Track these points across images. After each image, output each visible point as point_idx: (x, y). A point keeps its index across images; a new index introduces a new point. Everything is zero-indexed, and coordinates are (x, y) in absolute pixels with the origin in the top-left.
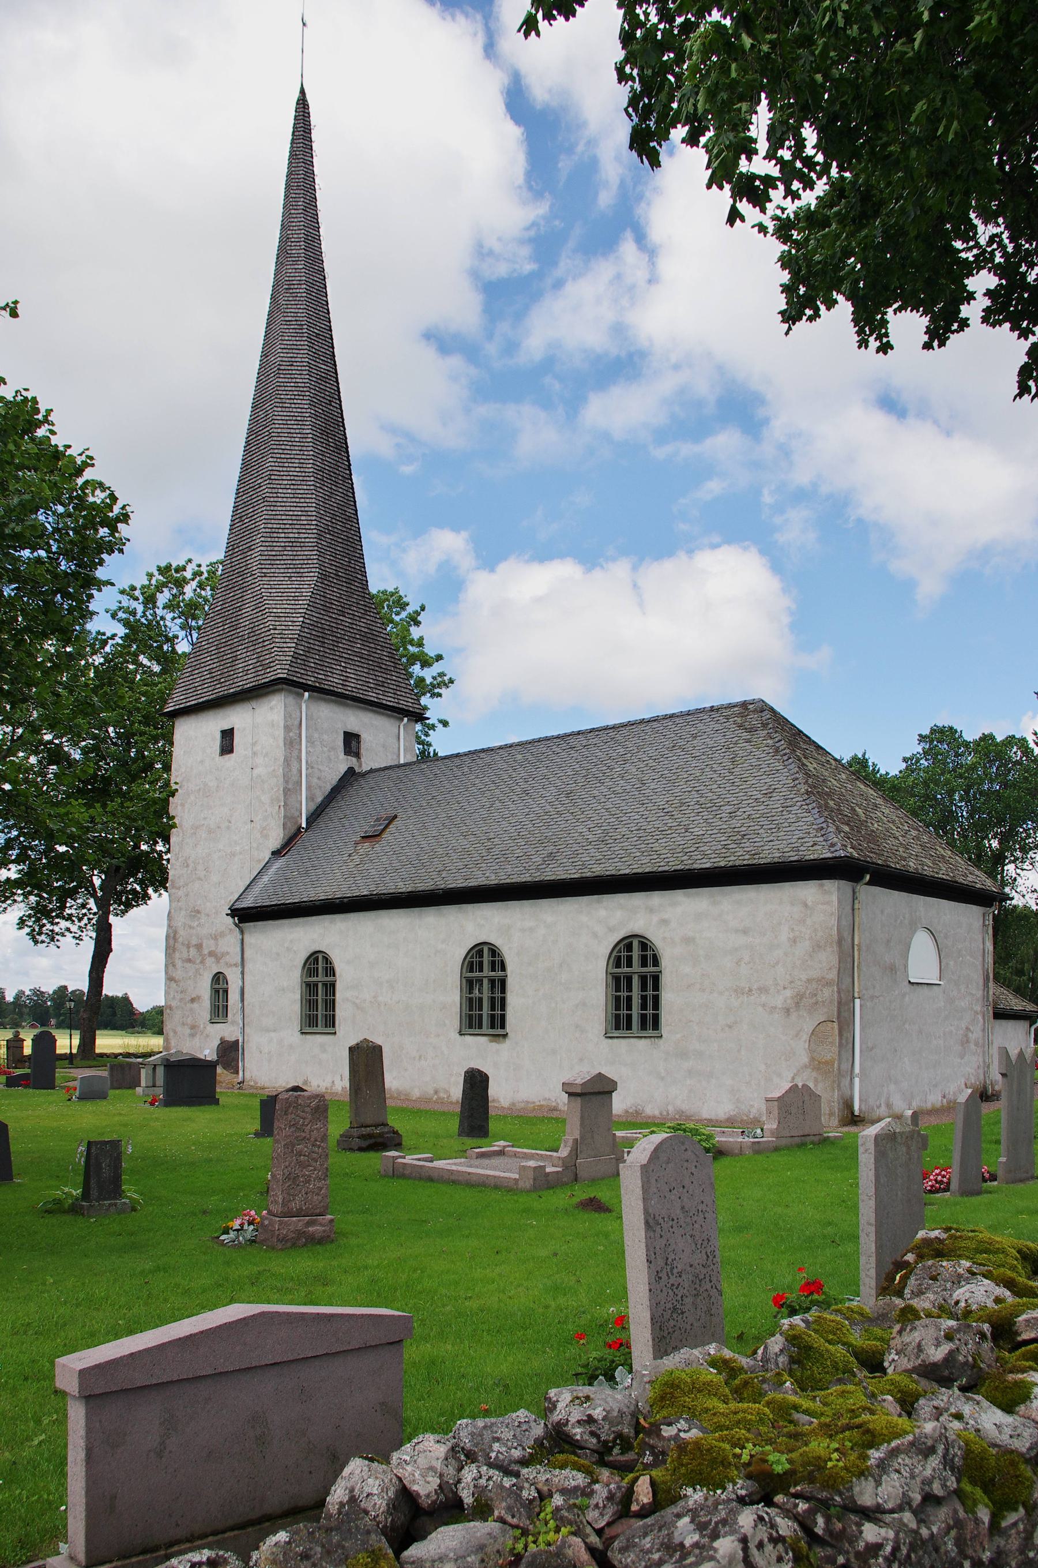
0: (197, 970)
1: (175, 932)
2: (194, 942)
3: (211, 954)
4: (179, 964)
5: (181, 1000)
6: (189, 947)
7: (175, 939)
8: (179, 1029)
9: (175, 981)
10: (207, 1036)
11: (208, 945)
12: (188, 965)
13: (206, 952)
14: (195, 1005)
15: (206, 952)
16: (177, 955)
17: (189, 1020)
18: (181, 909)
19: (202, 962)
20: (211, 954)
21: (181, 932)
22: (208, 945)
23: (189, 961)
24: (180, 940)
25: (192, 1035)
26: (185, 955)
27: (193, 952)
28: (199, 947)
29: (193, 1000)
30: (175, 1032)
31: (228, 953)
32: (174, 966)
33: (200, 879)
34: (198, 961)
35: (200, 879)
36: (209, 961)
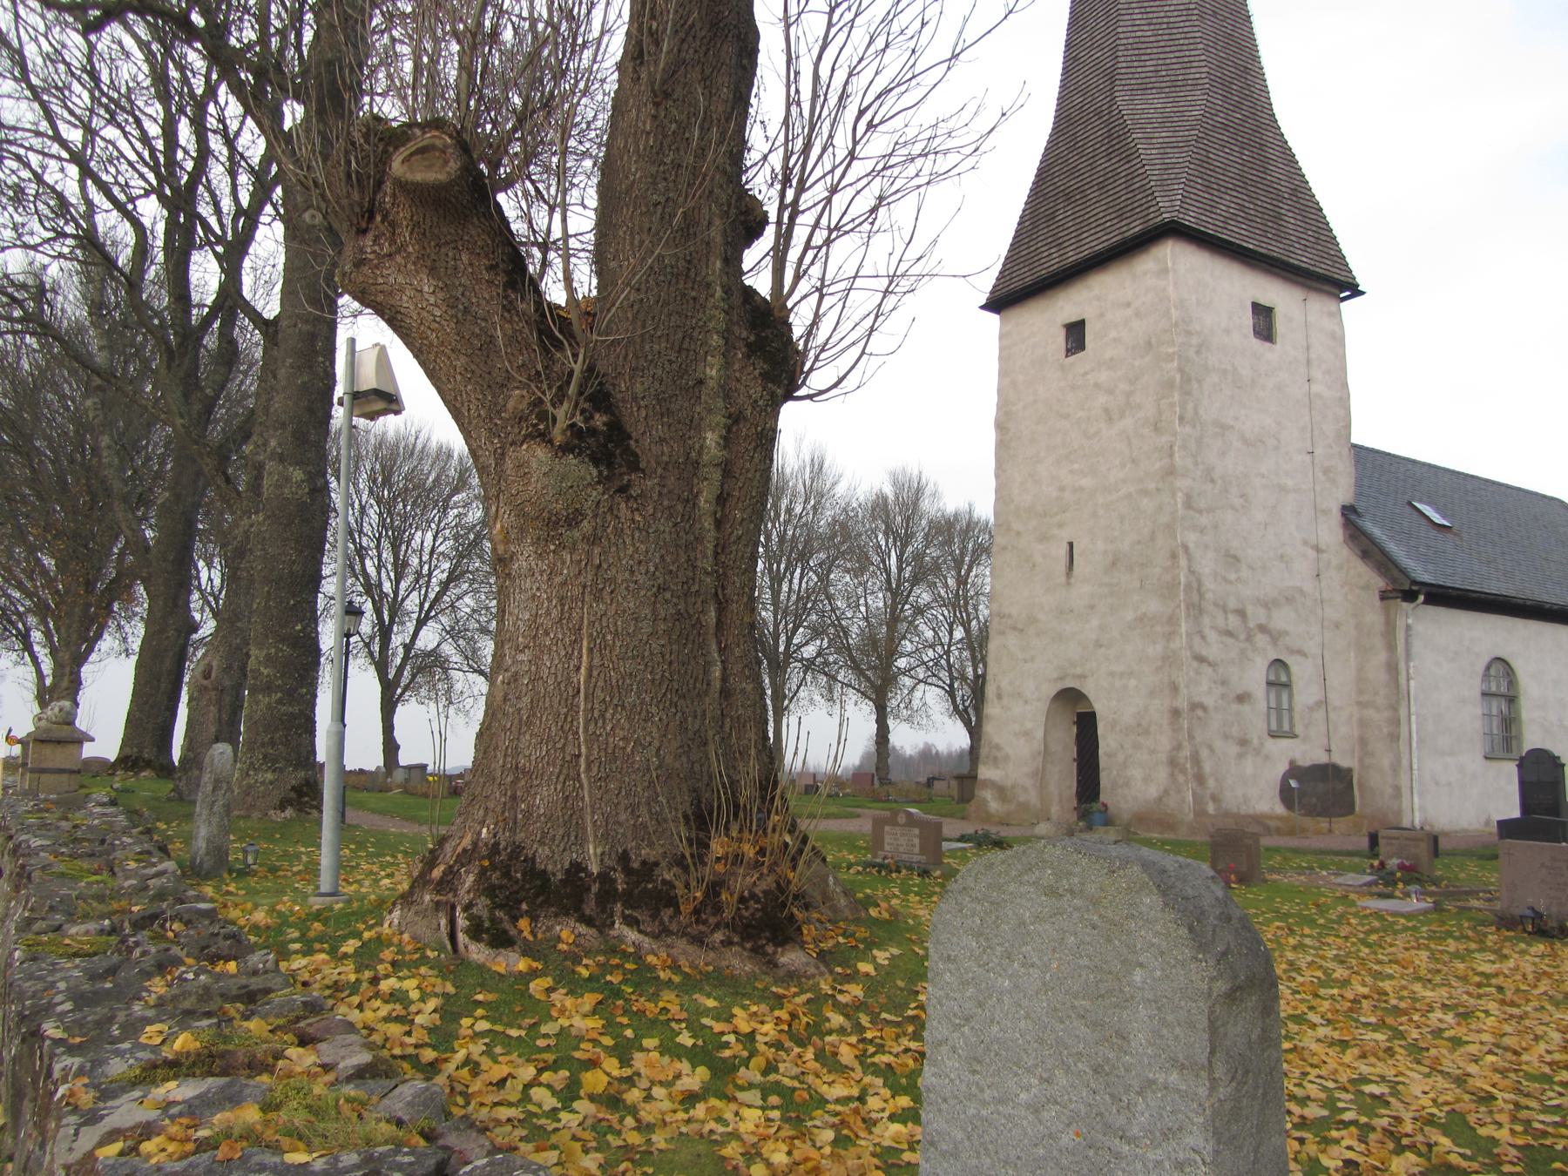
0: (1243, 652)
1: (1199, 582)
2: (1232, 604)
3: (1262, 628)
4: (1212, 636)
5: (1223, 696)
6: (1225, 612)
7: (1201, 595)
8: (1218, 744)
9: (1210, 664)
10: (1267, 757)
11: (1257, 615)
12: (1229, 641)
13: (1251, 625)
14: (1246, 708)
15: (1251, 625)
16: (1206, 621)
17: (1235, 731)
18: (1206, 547)
19: (1249, 639)
20: (1262, 628)
21: (1209, 584)
22: (1257, 615)
23: (1229, 634)
24: (1209, 596)
25: (1240, 756)
26: (1220, 622)
27: (1233, 622)
28: (1242, 613)
29: (1242, 698)
30: (1211, 748)
31: (1286, 633)
32: (1203, 637)
33: (1233, 508)
34: (1242, 637)
35: (1233, 508)
36: (1261, 640)
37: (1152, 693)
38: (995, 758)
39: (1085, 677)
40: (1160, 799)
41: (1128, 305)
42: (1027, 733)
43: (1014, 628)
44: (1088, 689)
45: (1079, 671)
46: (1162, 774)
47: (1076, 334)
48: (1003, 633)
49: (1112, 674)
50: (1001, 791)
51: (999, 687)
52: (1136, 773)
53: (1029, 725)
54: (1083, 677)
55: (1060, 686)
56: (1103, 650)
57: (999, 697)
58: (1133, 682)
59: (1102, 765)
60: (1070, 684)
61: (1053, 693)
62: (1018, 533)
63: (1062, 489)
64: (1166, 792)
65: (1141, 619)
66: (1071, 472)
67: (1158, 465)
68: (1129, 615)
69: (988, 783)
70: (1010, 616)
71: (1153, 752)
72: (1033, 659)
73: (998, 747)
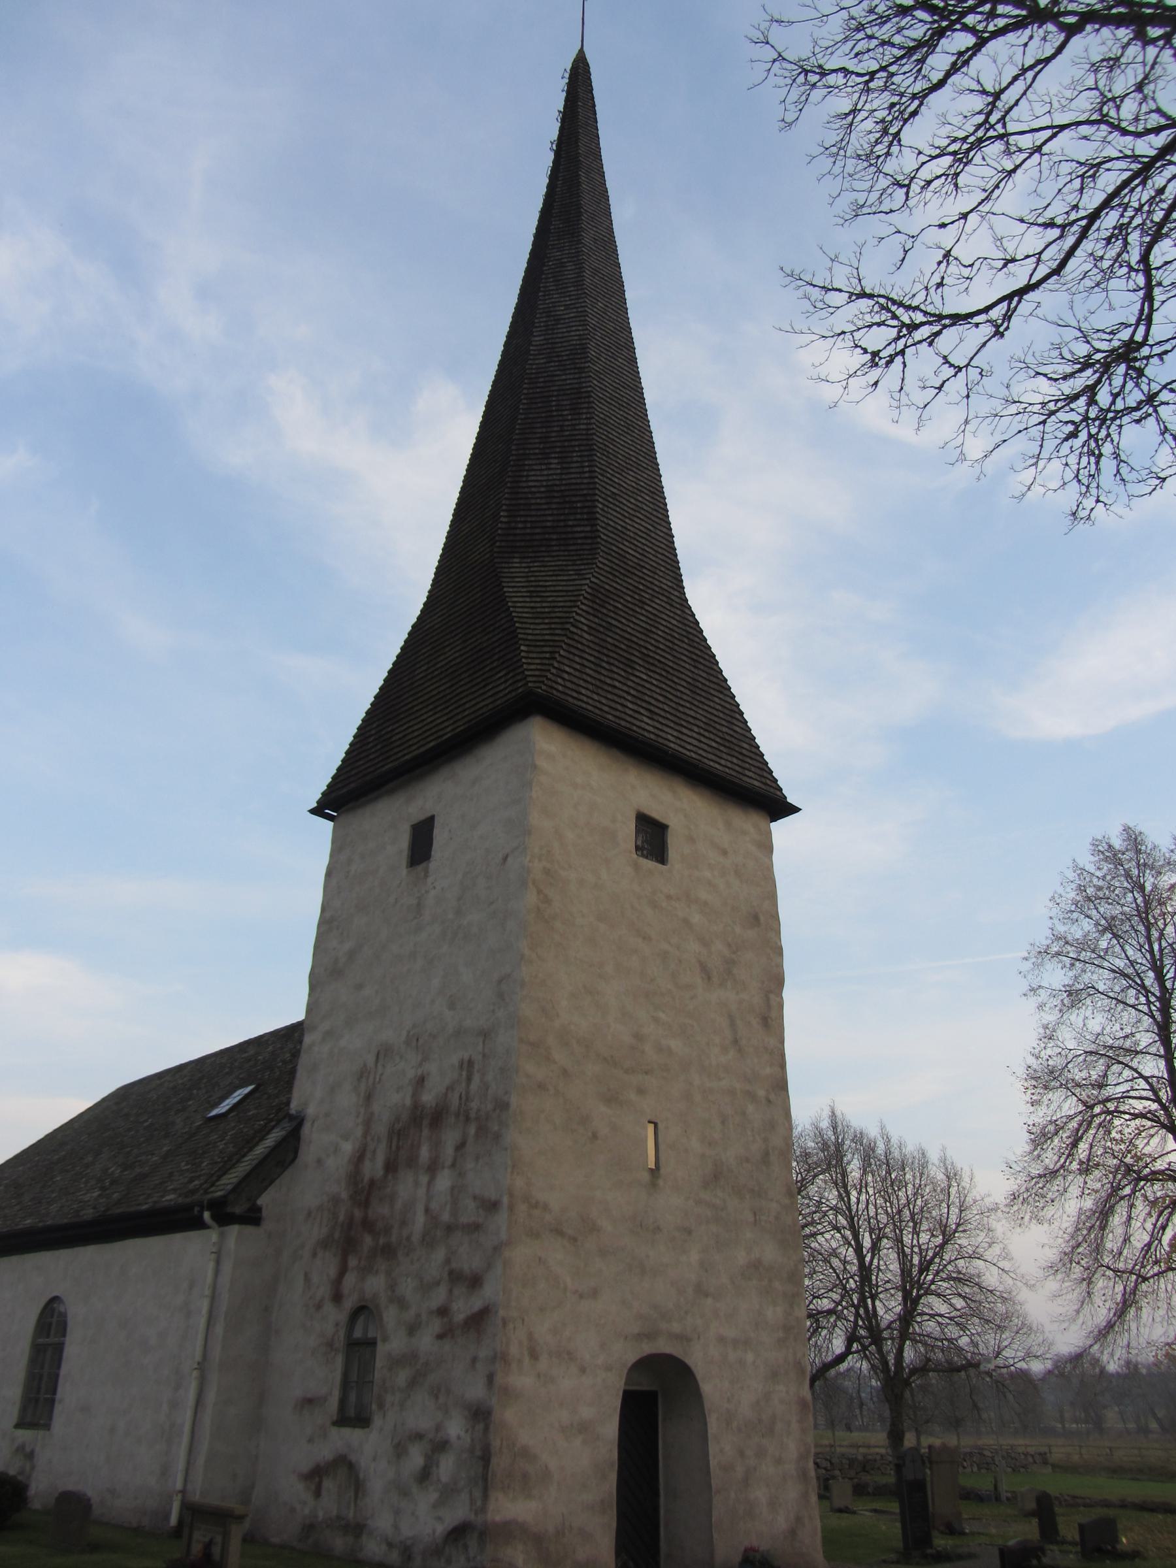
37: (774, 1375)
38: (525, 1476)
39: (689, 1340)
40: (793, 1533)
41: (725, 853)
42: (583, 1428)
43: (558, 1232)
44: (696, 1359)
45: (676, 1327)
46: (792, 1492)
47: (652, 837)
48: (534, 1235)
49: (722, 1340)
50: (537, 1540)
51: (530, 1336)
52: (760, 1494)
53: (587, 1413)
54: (682, 1338)
55: (647, 1349)
56: (709, 1301)
57: (534, 1355)
58: (750, 1357)
59: (715, 1483)
60: (663, 1346)
61: (632, 1358)
62: (565, 1072)
63: (639, 1037)
64: (799, 1519)
65: (756, 1266)
66: (656, 1020)
67: (768, 1070)
68: (741, 1257)
69: (509, 1531)
70: (546, 1207)
71: (779, 1461)
72: (594, 1293)
73: (526, 1453)
